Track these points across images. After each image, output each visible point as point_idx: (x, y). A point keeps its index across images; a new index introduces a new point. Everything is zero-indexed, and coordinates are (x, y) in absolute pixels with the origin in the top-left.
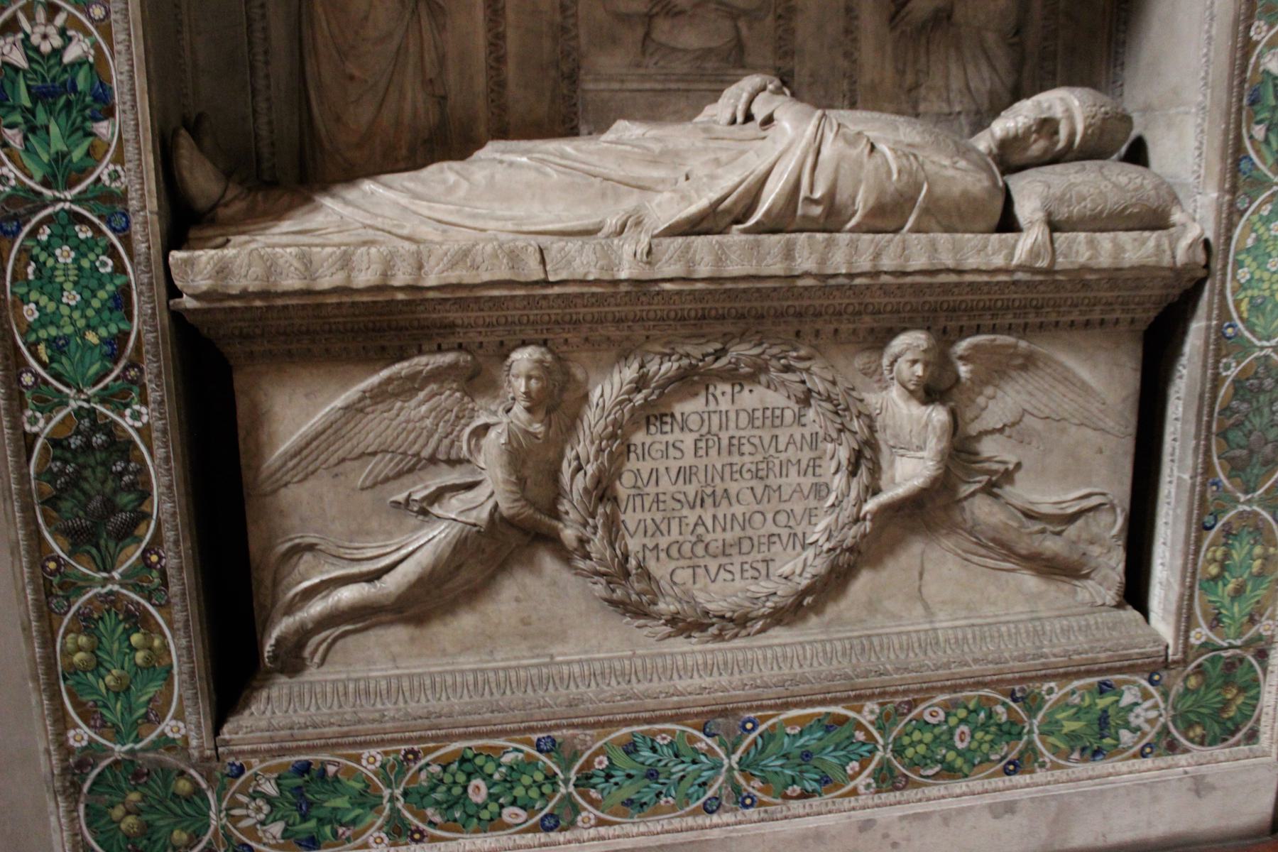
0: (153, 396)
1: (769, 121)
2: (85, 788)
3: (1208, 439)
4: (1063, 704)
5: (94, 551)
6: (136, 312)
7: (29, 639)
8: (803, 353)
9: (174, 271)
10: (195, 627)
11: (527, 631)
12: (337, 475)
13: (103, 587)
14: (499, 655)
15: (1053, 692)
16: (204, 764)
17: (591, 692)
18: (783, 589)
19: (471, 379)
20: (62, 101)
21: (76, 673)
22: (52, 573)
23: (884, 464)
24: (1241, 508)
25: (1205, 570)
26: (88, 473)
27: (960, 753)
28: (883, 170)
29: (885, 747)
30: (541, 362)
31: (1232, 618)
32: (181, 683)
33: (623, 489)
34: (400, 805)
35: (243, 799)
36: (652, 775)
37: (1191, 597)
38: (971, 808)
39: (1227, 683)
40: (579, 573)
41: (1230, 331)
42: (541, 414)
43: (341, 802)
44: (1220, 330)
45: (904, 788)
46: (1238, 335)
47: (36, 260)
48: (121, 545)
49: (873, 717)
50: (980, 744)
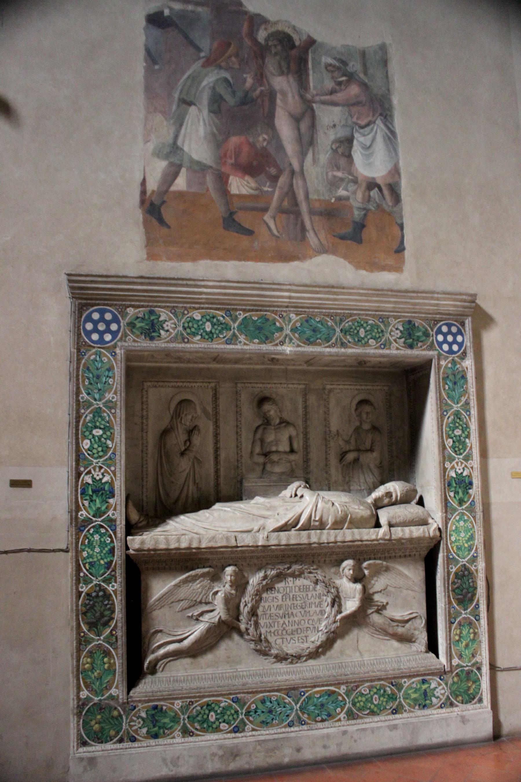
0: (119, 580)
1: (302, 496)
3: (448, 592)
4: (410, 687)
5: (96, 630)
6: (116, 554)
7: (73, 659)
8: (315, 567)
9: (128, 543)
10: (125, 656)
11: (230, 661)
12: (170, 607)
14: (220, 669)
15: (406, 683)
16: (124, 705)
17: (250, 681)
18: (312, 646)
19: (213, 576)
20: (101, 493)
22: (82, 637)
23: (343, 603)
24: (464, 616)
25: (454, 638)
26: (96, 604)
27: (375, 706)
28: (336, 512)
29: (349, 703)
30: (235, 571)
31: (466, 655)
32: (119, 675)
33: (260, 612)
34: (186, 721)
35: (135, 719)
36: (270, 712)
37: (450, 647)
38: (381, 727)
39: (468, 680)
40: (246, 640)
41: (451, 557)
42: (234, 588)
43: (167, 720)
44: (448, 556)
45: (357, 719)
46: (454, 557)
47: (88, 538)
49: (344, 691)
50: (382, 702)
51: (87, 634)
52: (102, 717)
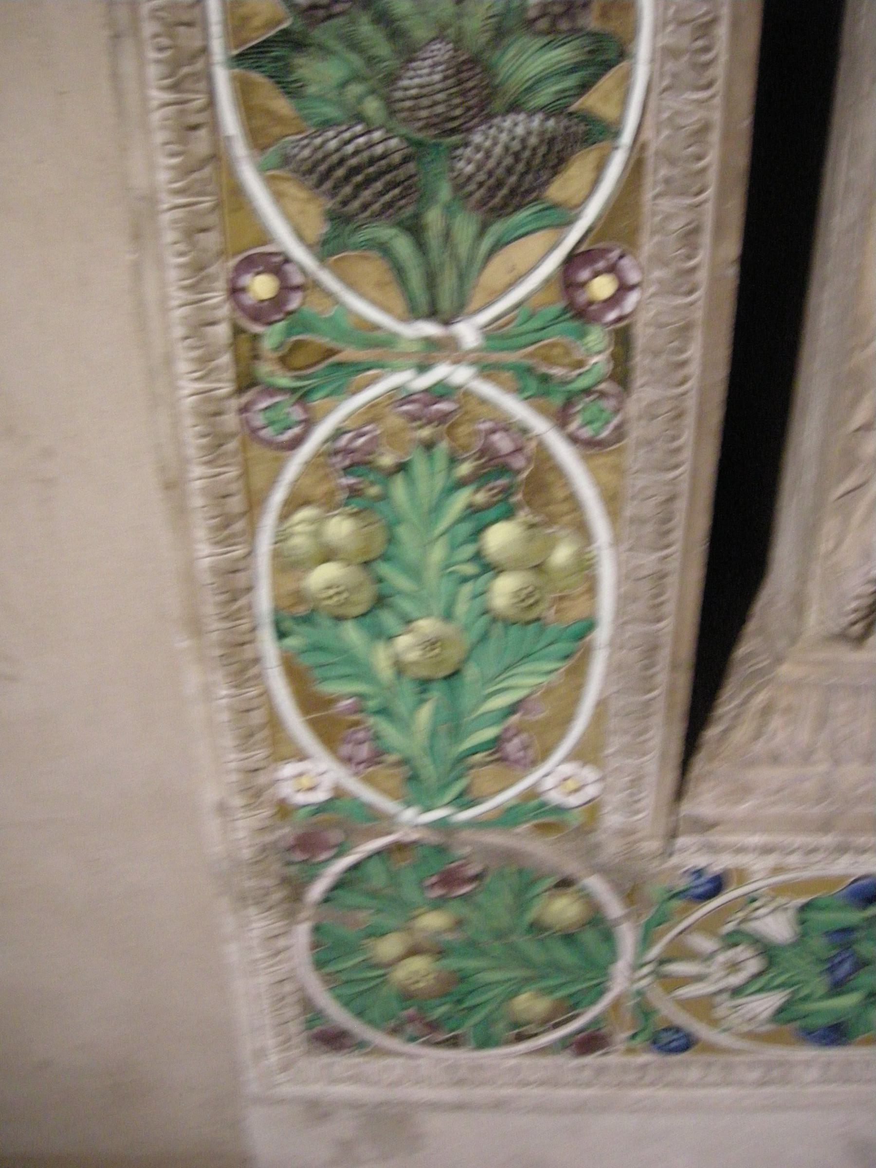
5: (403, 246)
13: (423, 368)
21: (307, 620)
32: (615, 669)
48: (497, 229)
51: (310, 286)
52: (459, 924)
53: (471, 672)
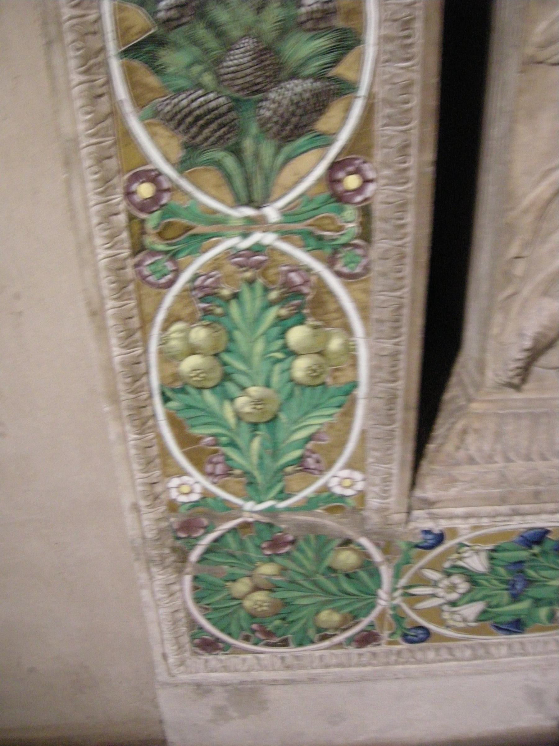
2: (194, 556)
5: (230, 162)
7: (102, 329)
13: (245, 235)
21: (182, 390)
32: (371, 411)
48: (287, 149)
51: (174, 189)
52: (284, 570)
53: (283, 417)
